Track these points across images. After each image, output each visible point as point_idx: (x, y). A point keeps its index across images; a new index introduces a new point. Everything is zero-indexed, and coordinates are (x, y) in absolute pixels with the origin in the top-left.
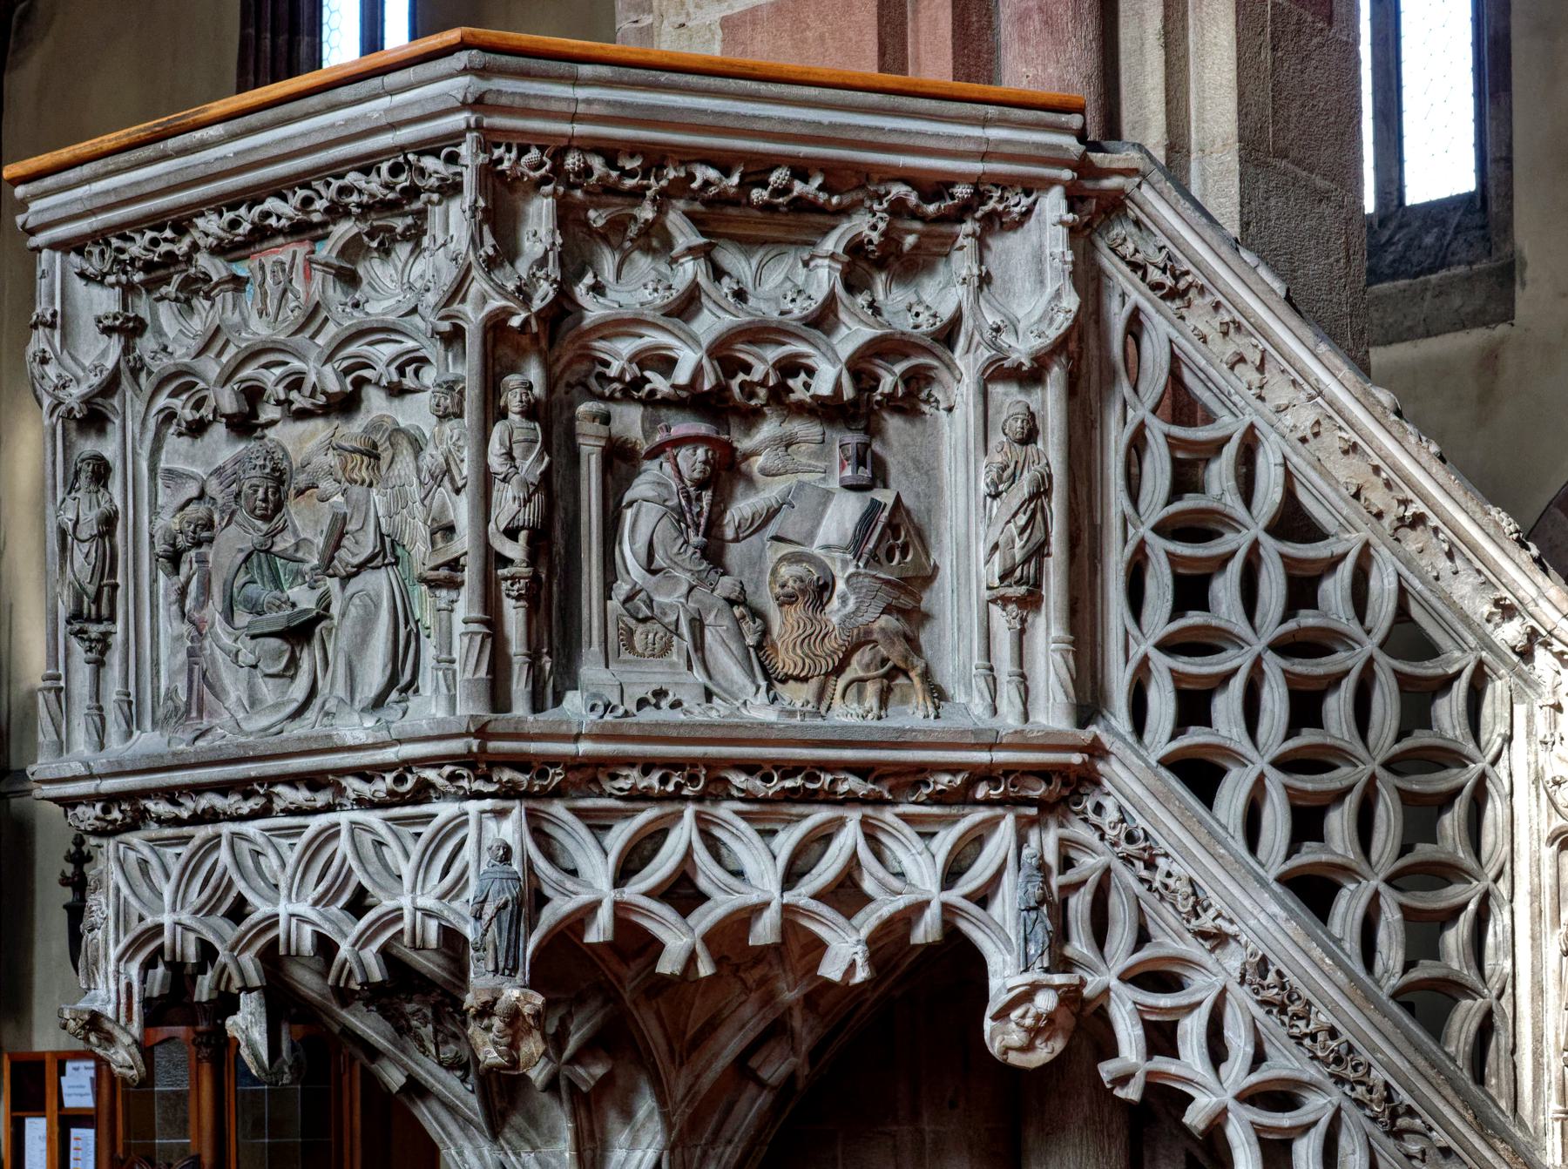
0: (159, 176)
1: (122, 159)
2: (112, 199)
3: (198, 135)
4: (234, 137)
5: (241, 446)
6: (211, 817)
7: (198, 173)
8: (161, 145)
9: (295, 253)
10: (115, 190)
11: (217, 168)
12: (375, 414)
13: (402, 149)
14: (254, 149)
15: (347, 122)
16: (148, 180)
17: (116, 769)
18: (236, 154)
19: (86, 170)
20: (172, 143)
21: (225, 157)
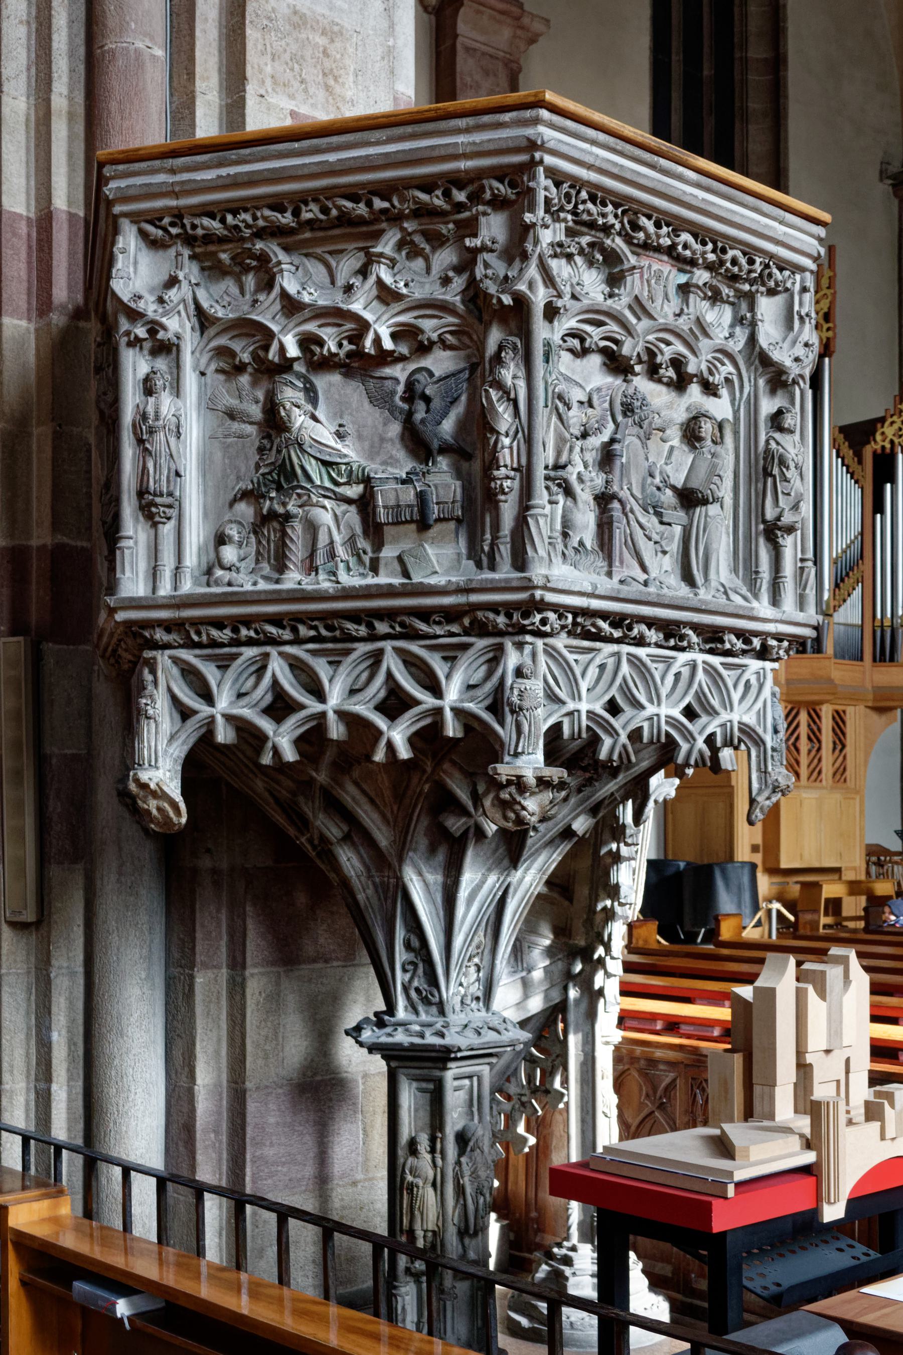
0: (653, 179)
1: (629, 148)
2: (615, 170)
3: (680, 169)
4: (698, 186)
5: (609, 379)
6: (598, 637)
7: (676, 194)
8: (656, 158)
9: (670, 271)
10: (622, 166)
11: (687, 199)
12: (693, 400)
13: (772, 256)
14: (713, 204)
15: (766, 226)
16: (645, 176)
17: (614, 595)
18: (703, 200)
19: (602, 137)
20: (663, 162)
21: (696, 197)
